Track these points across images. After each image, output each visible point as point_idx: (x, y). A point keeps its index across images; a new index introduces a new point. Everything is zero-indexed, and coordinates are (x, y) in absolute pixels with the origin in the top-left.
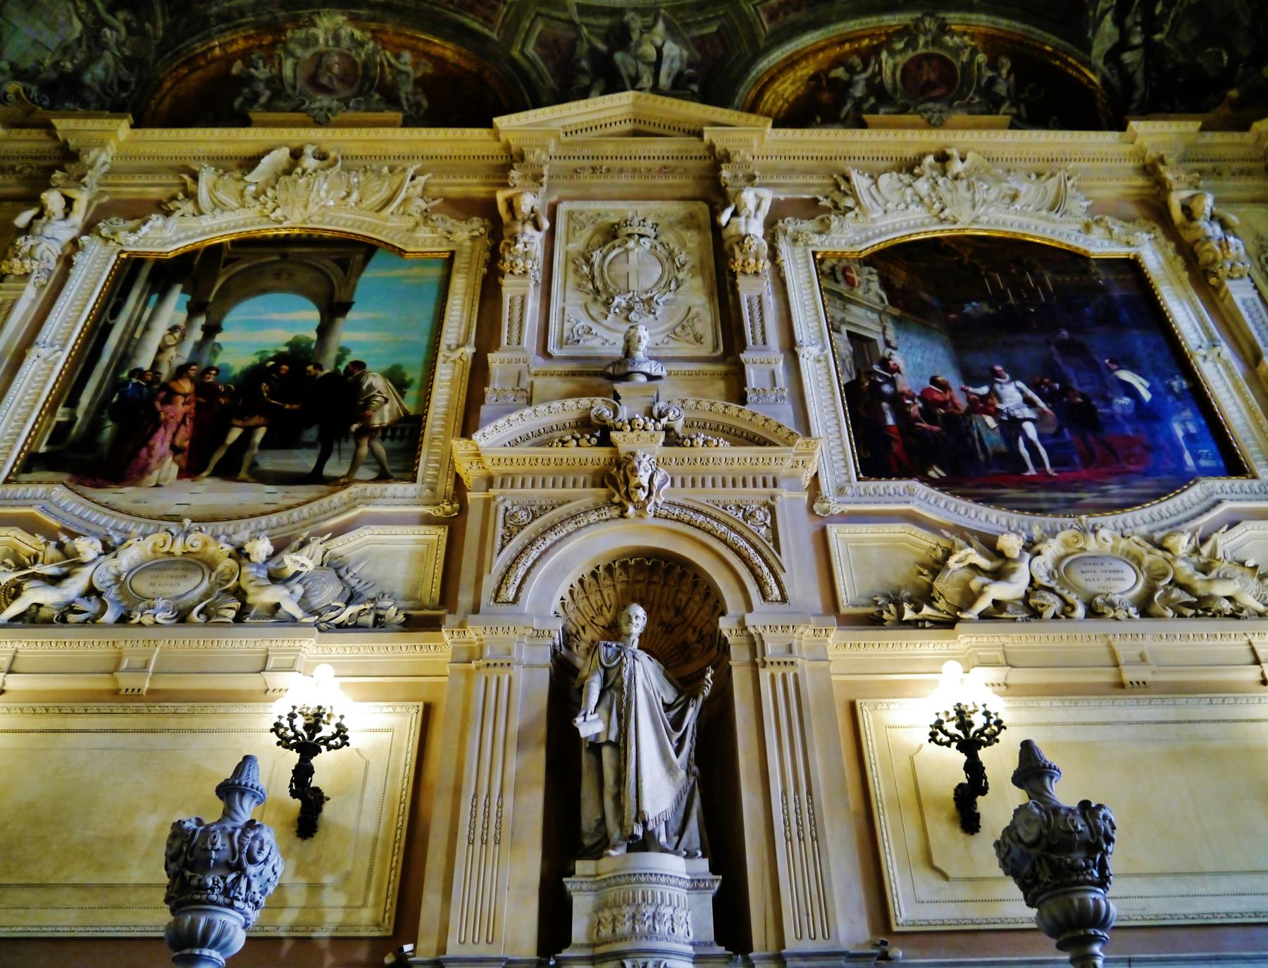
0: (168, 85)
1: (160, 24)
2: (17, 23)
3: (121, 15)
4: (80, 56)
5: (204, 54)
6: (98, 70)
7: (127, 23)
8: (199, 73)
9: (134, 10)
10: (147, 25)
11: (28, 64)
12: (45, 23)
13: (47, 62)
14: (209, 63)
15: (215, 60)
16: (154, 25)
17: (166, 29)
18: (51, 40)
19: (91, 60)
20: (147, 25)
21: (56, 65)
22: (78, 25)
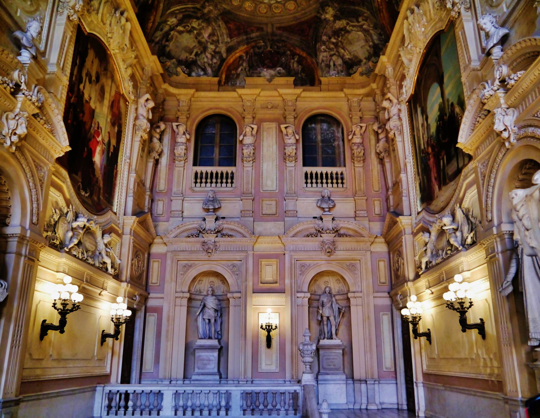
0: (384, 23)
1: (366, 11)
2: (354, 49)
3: (360, 19)
4: (369, 38)
5: (378, 4)
6: (375, 37)
7: (363, 20)
8: (384, 10)
9: (360, 16)
10: (365, 15)
11: (367, 55)
12: (357, 42)
13: (368, 48)
14: (382, 5)
15: (381, 3)
16: (365, 13)
17: (368, 10)
18: (362, 43)
19: (371, 36)
20: (365, 15)
21: (370, 46)
22: (360, 33)
